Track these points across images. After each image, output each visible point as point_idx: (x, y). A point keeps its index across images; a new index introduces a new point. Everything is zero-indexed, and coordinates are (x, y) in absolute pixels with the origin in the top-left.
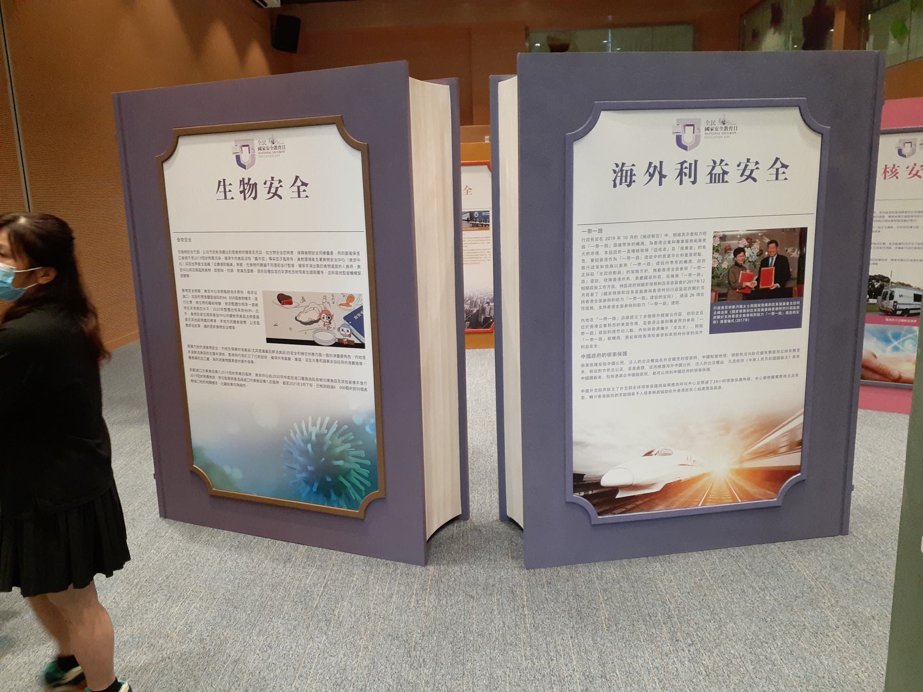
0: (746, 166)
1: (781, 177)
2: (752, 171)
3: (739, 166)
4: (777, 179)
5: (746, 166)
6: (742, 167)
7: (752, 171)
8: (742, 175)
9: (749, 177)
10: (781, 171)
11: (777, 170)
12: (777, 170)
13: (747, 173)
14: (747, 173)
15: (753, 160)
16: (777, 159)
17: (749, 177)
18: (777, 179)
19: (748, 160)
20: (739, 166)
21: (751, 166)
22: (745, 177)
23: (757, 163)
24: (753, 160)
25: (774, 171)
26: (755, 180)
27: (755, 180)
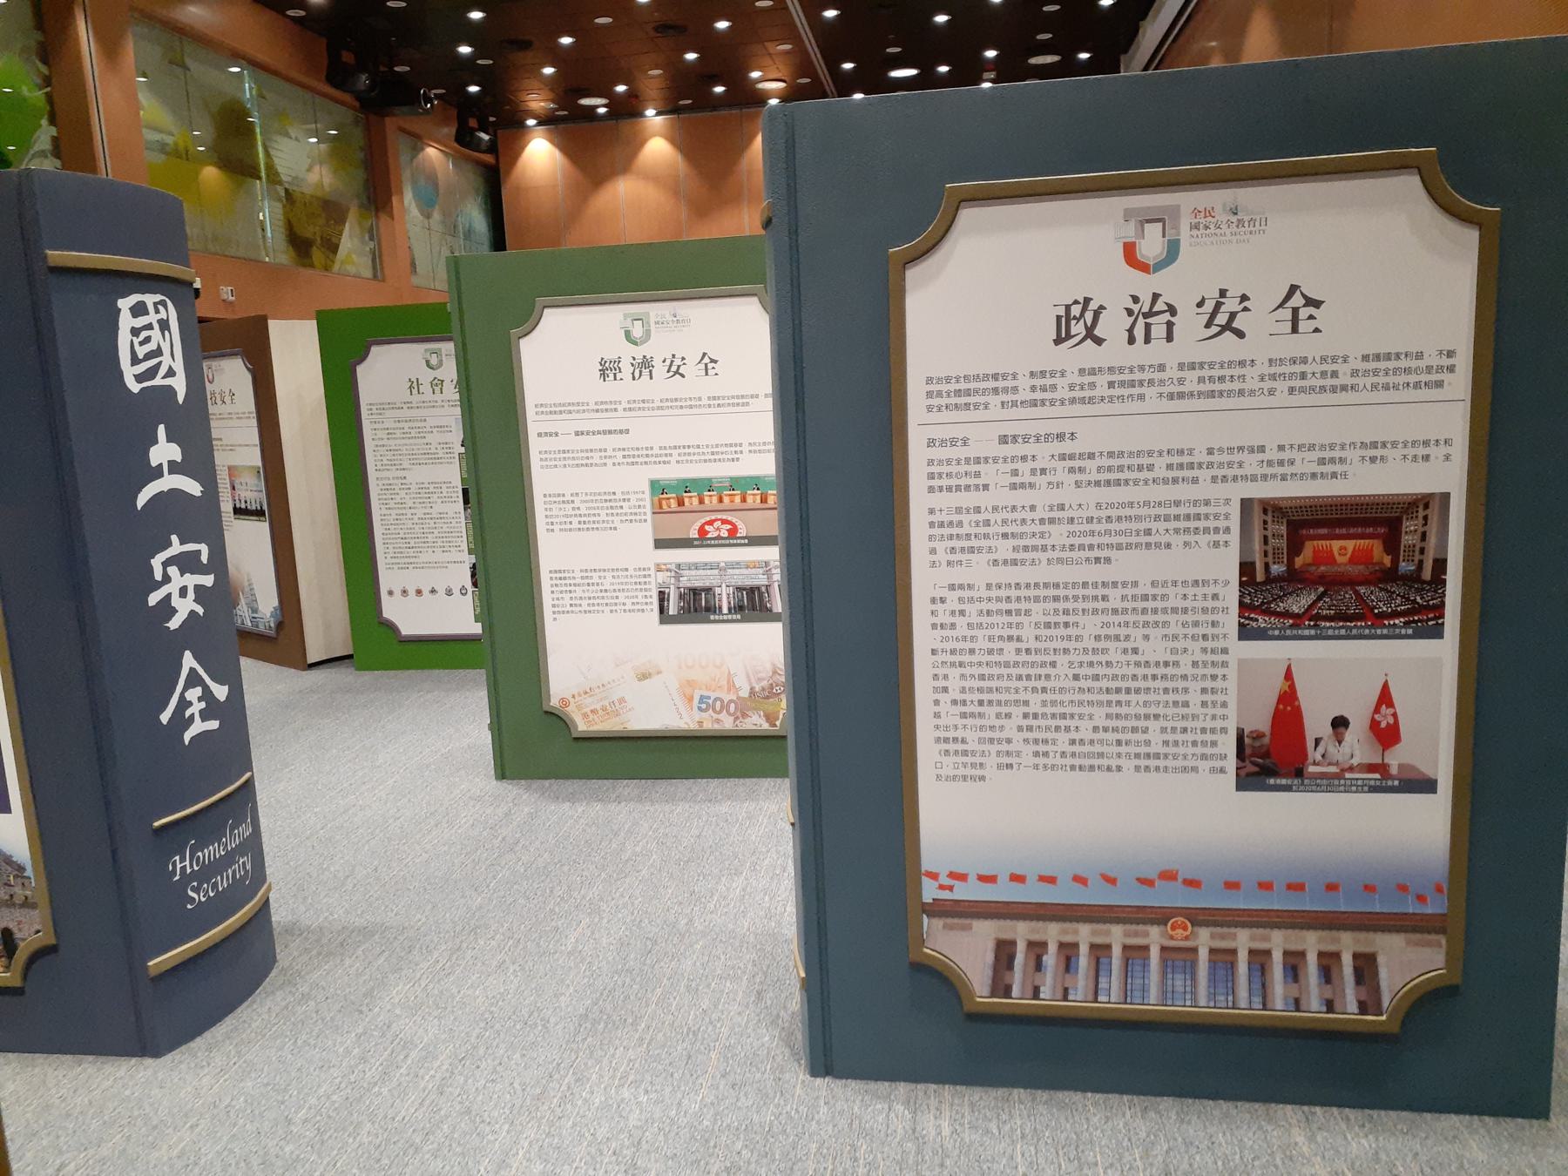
0: (1218, 305)
1: (1302, 326)
2: (1233, 315)
3: (1200, 304)
4: (1295, 330)
5: (1218, 305)
6: (1209, 306)
7: (1233, 315)
8: (1208, 325)
9: (1227, 327)
10: (1304, 313)
11: (1295, 311)
12: (1295, 311)
13: (1221, 319)
14: (1221, 319)
15: (1234, 292)
16: (1293, 289)
17: (1227, 327)
18: (1295, 330)
19: (1223, 293)
20: (1200, 304)
21: (1231, 305)
22: (1214, 330)
23: (1244, 298)
24: (1234, 292)
25: (1286, 314)
26: (1240, 334)
27: (1240, 334)
